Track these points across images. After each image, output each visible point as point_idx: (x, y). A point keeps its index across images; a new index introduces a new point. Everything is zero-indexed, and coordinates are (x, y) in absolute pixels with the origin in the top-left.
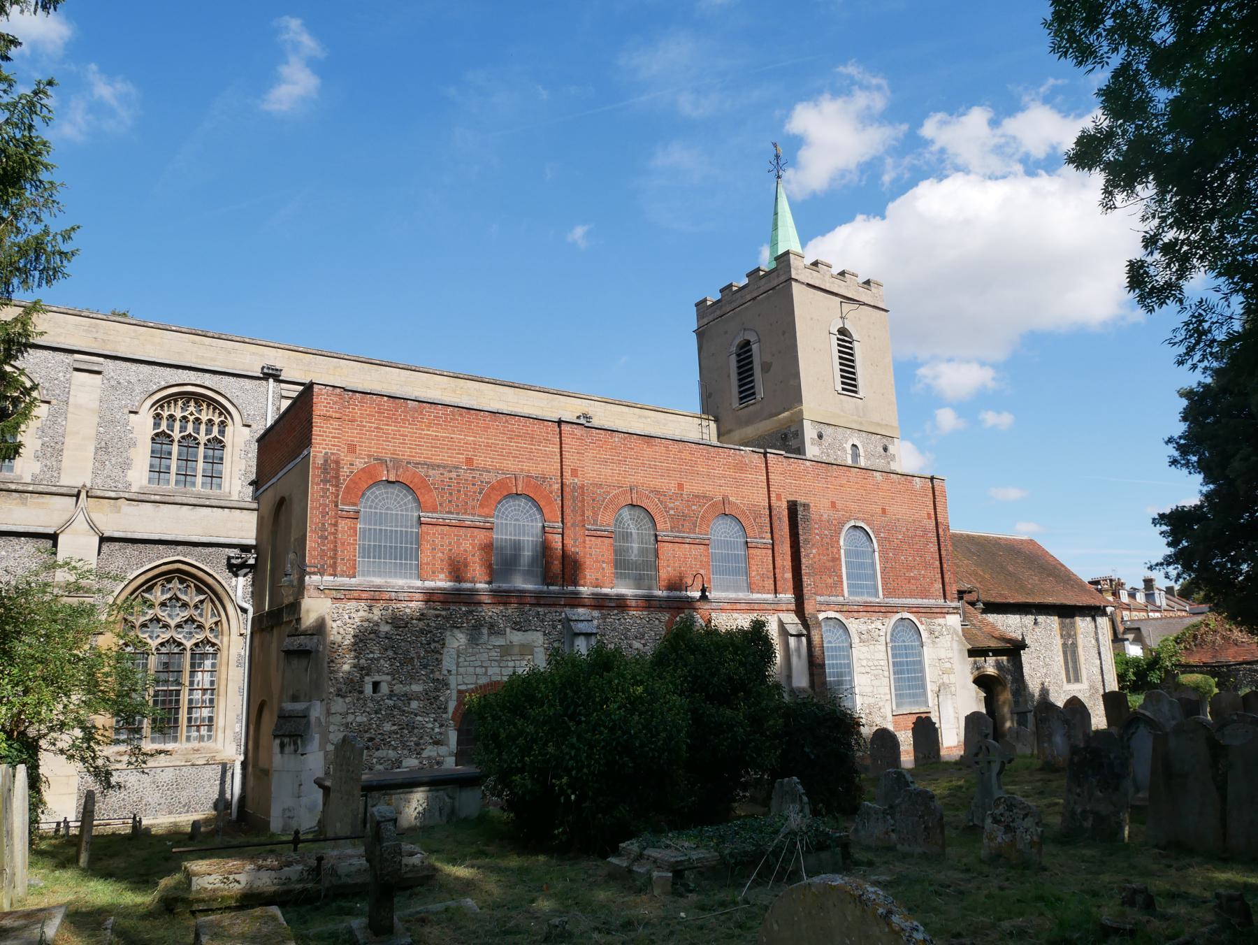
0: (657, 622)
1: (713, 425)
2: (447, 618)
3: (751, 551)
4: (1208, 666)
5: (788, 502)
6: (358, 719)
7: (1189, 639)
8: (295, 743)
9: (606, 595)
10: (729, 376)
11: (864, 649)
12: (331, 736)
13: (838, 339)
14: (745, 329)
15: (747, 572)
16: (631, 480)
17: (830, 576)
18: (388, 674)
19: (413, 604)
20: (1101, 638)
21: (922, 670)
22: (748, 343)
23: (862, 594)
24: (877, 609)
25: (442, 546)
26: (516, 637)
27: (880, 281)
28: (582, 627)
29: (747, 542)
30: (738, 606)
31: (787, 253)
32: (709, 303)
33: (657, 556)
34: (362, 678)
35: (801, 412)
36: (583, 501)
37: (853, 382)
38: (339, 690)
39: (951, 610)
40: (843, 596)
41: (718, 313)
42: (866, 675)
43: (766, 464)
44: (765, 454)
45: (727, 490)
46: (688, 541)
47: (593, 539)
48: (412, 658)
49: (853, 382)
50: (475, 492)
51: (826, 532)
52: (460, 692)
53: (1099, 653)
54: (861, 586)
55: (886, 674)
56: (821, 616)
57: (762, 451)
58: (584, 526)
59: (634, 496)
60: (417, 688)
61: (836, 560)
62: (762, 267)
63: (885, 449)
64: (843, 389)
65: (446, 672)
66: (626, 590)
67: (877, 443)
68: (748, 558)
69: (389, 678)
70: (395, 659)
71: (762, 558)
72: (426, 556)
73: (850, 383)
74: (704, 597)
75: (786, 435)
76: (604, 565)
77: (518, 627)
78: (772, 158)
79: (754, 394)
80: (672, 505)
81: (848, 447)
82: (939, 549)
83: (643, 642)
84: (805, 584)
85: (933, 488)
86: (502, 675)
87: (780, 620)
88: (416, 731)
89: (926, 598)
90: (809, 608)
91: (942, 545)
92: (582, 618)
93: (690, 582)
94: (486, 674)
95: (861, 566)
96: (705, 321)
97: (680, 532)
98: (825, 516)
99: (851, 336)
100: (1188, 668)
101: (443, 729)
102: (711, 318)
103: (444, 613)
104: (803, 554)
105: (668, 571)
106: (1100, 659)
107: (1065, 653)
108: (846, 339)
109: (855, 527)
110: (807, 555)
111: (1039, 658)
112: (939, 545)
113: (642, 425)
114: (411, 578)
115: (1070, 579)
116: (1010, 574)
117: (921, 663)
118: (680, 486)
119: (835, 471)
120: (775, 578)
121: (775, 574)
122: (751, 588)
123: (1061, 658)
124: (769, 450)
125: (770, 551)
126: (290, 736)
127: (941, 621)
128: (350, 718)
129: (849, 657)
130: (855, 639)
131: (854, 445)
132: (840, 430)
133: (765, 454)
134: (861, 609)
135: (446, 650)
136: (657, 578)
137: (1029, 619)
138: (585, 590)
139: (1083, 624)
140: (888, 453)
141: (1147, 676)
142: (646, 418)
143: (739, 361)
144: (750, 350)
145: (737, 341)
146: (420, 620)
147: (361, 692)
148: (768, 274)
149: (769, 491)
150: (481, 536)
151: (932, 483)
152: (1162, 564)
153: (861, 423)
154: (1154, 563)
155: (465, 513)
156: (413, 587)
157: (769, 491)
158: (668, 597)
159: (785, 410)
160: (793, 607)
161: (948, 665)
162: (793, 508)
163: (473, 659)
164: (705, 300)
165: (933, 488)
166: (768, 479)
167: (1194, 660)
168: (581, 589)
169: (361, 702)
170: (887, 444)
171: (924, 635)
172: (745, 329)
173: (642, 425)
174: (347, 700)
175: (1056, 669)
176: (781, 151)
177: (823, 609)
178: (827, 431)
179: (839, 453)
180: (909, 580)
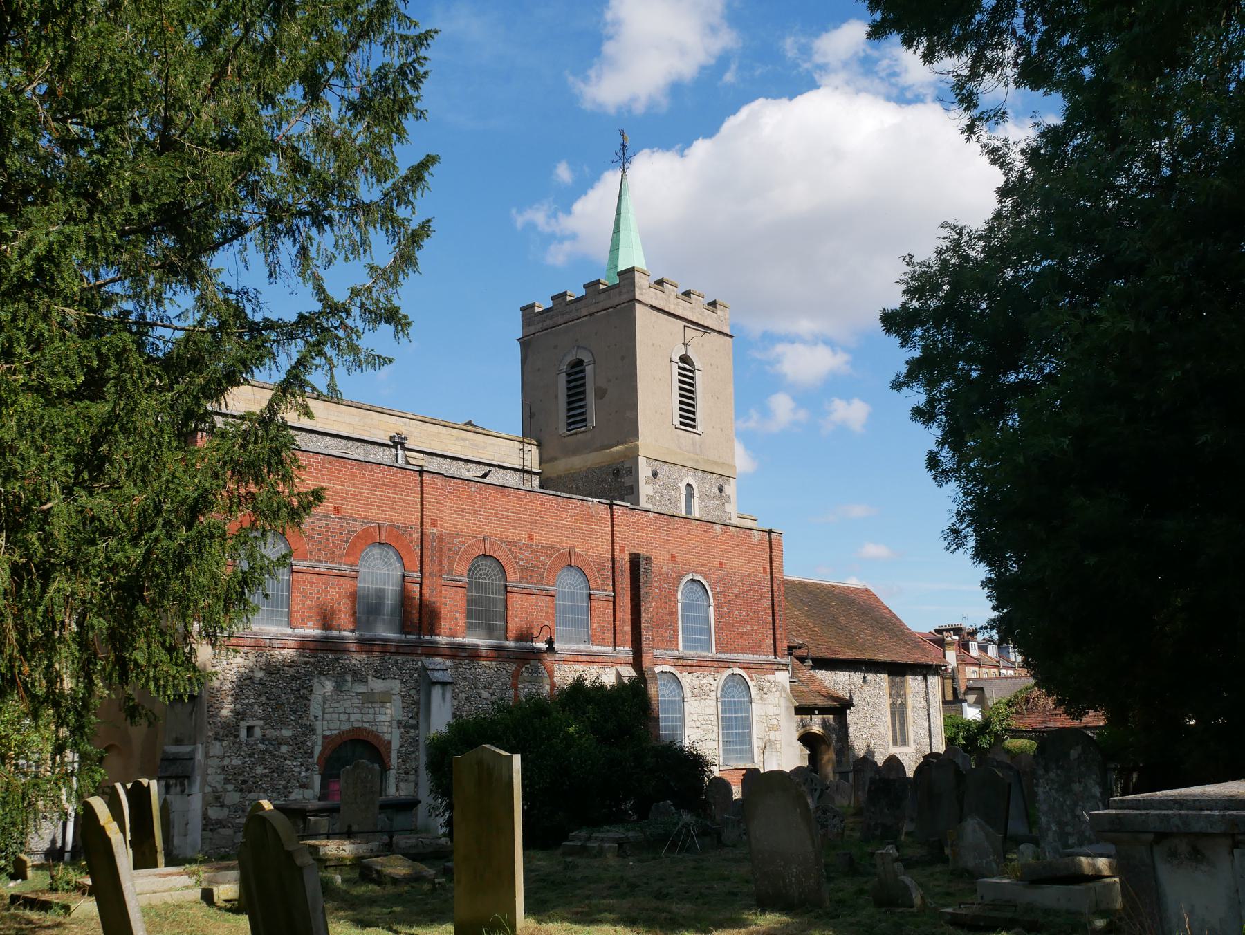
0: (504, 672)
1: (535, 450)
2: (315, 665)
3: (594, 603)
4: (1036, 732)
5: (631, 554)
6: (234, 762)
7: (1019, 703)
8: (182, 784)
9: (459, 644)
10: (556, 397)
11: (696, 704)
12: (209, 779)
13: (680, 368)
14: (578, 347)
15: (589, 626)
16: (485, 530)
17: (666, 630)
18: (261, 719)
19: (285, 651)
20: (931, 698)
21: (750, 726)
22: (580, 362)
23: (696, 648)
24: (710, 664)
25: (311, 594)
26: (378, 685)
27: (726, 304)
28: (438, 676)
29: (590, 594)
30: (580, 658)
31: (632, 270)
32: (537, 310)
33: (506, 607)
34: (238, 722)
35: (637, 447)
36: (441, 551)
37: (692, 416)
38: (217, 734)
39: (781, 667)
41: (548, 323)
43: (612, 515)
44: (611, 505)
45: (573, 542)
46: (535, 592)
47: (448, 588)
48: (283, 704)
49: (692, 416)
50: (342, 541)
51: (665, 585)
52: (325, 737)
53: (929, 715)
54: (695, 640)
55: (715, 729)
56: (657, 669)
57: (608, 502)
58: (441, 576)
59: (488, 546)
60: (287, 733)
61: (673, 613)
62: (603, 280)
63: (721, 490)
64: (682, 423)
65: (313, 718)
66: (479, 641)
67: (712, 483)
68: (590, 610)
69: (261, 723)
70: (268, 704)
71: (603, 610)
72: (296, 604)
73: (688, 418)
74: (551, 649)
75: (618, 470)
76: (457, 615)
77: (379, 675)
78: (618, 148)
79: (585, 420)
80: (522, 556)
81: (683, 486)
82: (773, 605)
83: (491, 691)
84: (643, 638)
85: (770, 542)
86: (363, 722)
87: (618, 673)
88: (284, 774)
90: (646, 661)
91: (776, 600)
92: (438, 667)
93: (535, 633)
94: (348, 720)
95: (695, 620)
96: (532, 329)
97: (528, 583)
98: (665, 569)
99: (692, 365)
100: (1017, 733)
101: (309, 774)
102: (539, 326)
103: (312, 660)
104: (643, 608)
105: (516, 623)
106: (929, 721)
107: (893, 714)
108: (688, 367)
109: (692, 580)
110: (647, 609)
111: (865, 718)
112: (773, 600)
113: (459, 448)
114: (281, 625)
115: (904, 634)
116: (842, 628)
117: (748, 719)
118: (530, 537)
119: (676, 523)
120: (615, 630)
121: (614, 627)
122: (591, 640)
123: (889, 719)
124: (615, 502)
125: (611, 604)
126: (177, 777)
127: (770, 677)
128: (226, 761)
129: (681, 711)
130: (688, 694)
131: (689, 485)
132: (676, 467)
133: (611, 505)
134: (694, 663)
135: (313, 696)
136: (505, 630)
137: (857, 677)
138: (443, 639)
139: (914, 684)
141: (977, 740)
142: (463, 440)
143: (569, 382)
144: (583, 371)
145: (570, 358)
146: (290, 666)
147: (237, 736)
148: (609, 289)
149: (613, 543)
150: (346, 585)
151: (770, 537)
152: (986, 628)
153: (697, 461)
154: (979, 626)
155: (333, 562)
156: (285, 635)
157: (613, 543)
158: (516, 648)
159: (618, 444)
160: (630, 660)
161: (775, 722)
162: (635, 561)
163: (336, 705)
164: (533, 306)
165: (770, 542)
166: (612, 531)
167: (1024, 725)
168: (439, 638)
169: (237, 745)
170: (723, 483)
171: (754, 691)
172: (578, 347)
173: (459, 448)
174: (225, 743)
175: (882, 731)
176: (628, 142)
177: (659, 662)
178: (662, 470)
179: (673, 493)
180: (741, 635)
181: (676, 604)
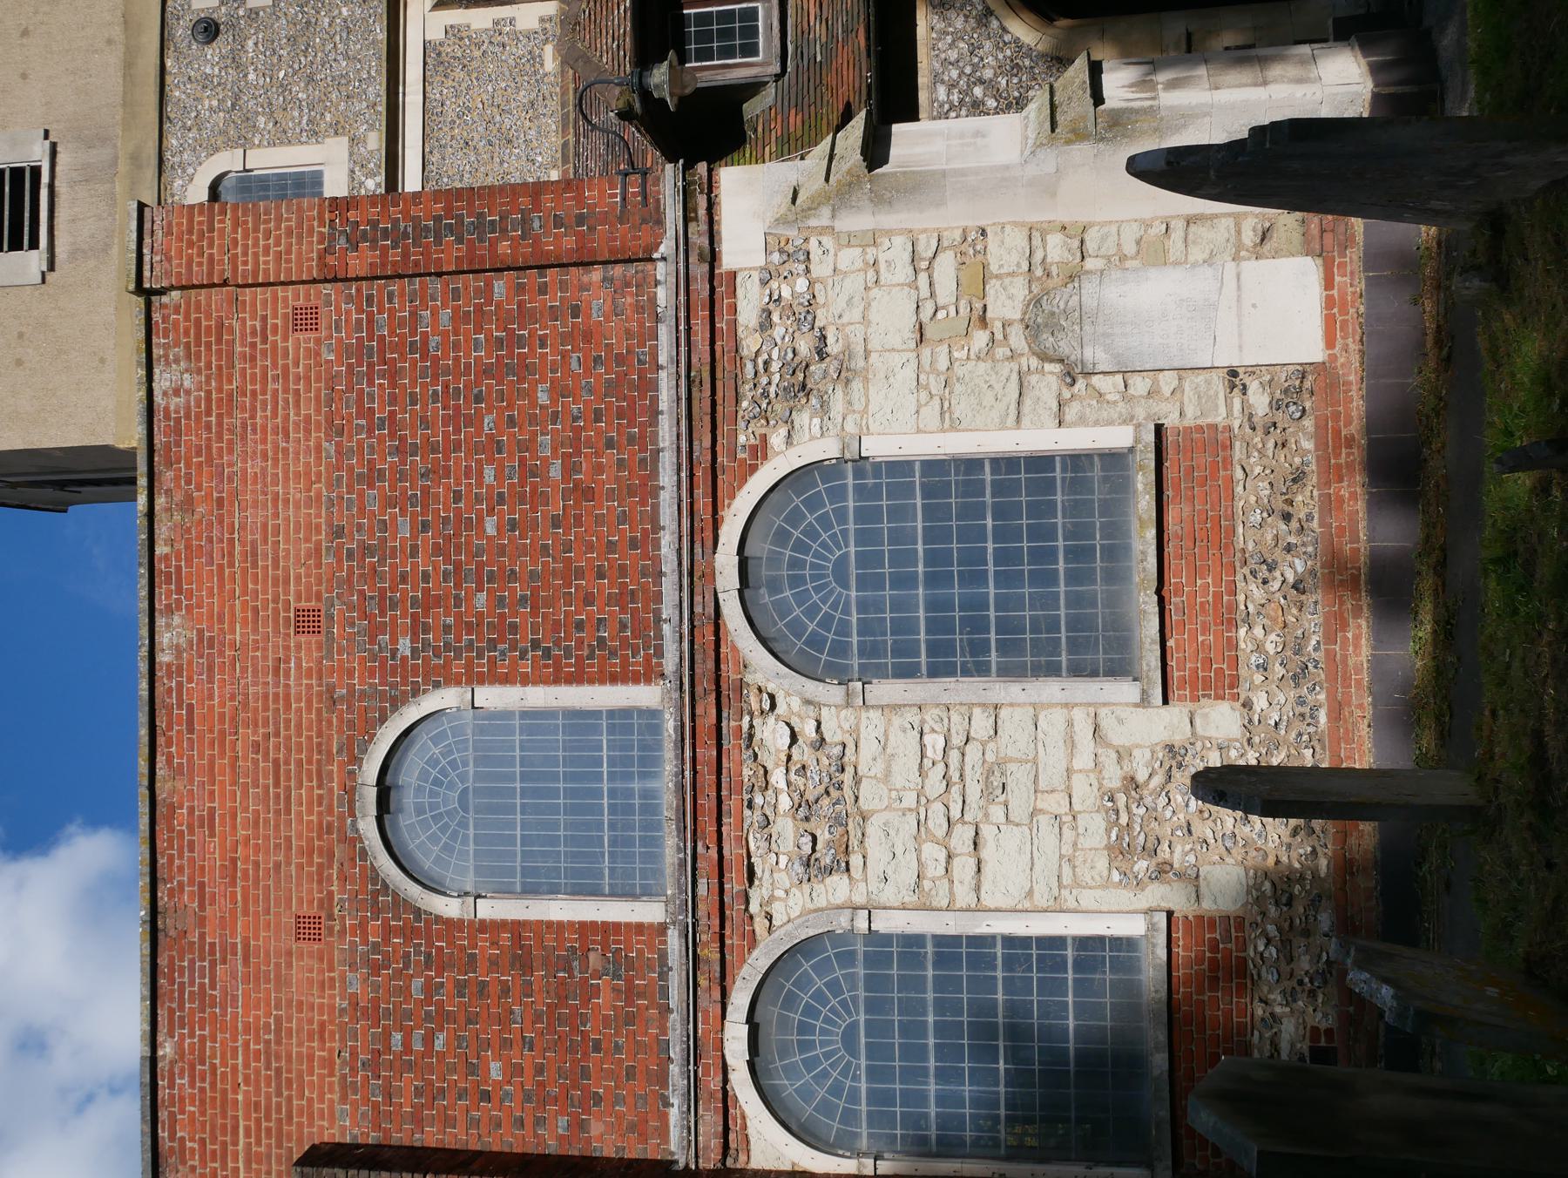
24: (707, 753)
39: (699, 240)
40: (662, 929)
42: (986, 853)
64: (34, 245)
89: (654, 386)
127: (748, 304)
140: (221, 15)
153: (135, 159)
177: (714, 1084)
181: (484, 926)
